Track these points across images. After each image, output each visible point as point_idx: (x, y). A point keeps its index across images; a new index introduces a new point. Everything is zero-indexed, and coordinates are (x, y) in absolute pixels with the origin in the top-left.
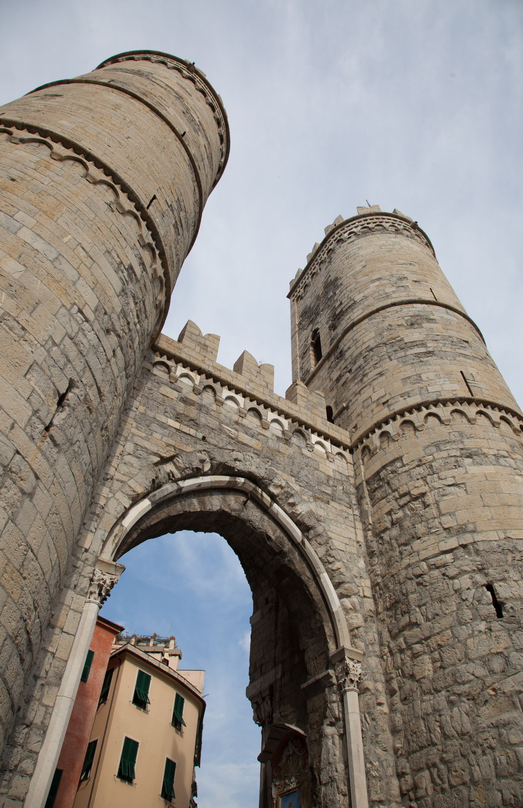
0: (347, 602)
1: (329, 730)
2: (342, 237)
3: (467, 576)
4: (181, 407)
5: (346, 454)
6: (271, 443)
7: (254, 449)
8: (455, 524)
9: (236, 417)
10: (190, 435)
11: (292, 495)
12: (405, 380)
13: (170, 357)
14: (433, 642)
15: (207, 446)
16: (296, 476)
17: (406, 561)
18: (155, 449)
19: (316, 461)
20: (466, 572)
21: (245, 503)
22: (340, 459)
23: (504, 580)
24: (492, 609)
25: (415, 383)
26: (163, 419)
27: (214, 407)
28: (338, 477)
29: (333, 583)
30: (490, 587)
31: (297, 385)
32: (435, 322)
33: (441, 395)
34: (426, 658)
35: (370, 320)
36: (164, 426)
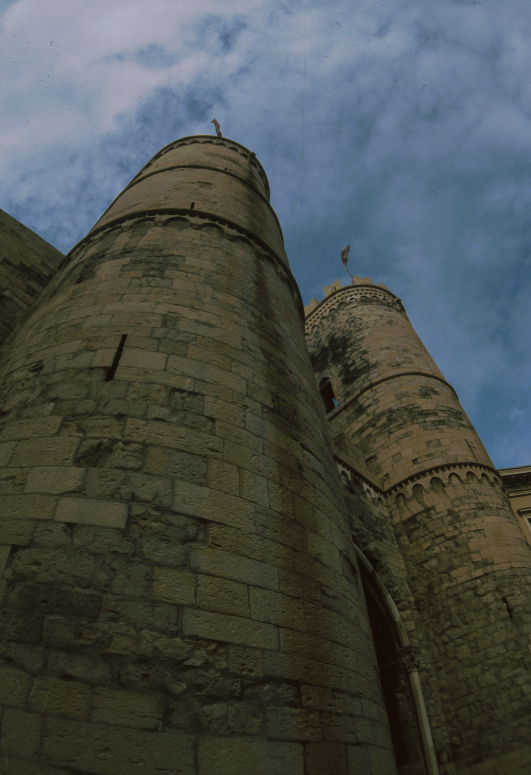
0: (405, 614)
1: (399, 695)
2: (344, 301)
3: (490, 594)
8: (480, 559)
12: (428, 443)
14: (470, 637)
17: (446, 585)
20: (490, 592)
23: (513, 595)
24: (506, 614)
25: (436, 447)
29: (394, 601)
30: (504, 600)
31: (344, 438)
33: (457, 459)
34: (465, 647)
35: (388, 384)
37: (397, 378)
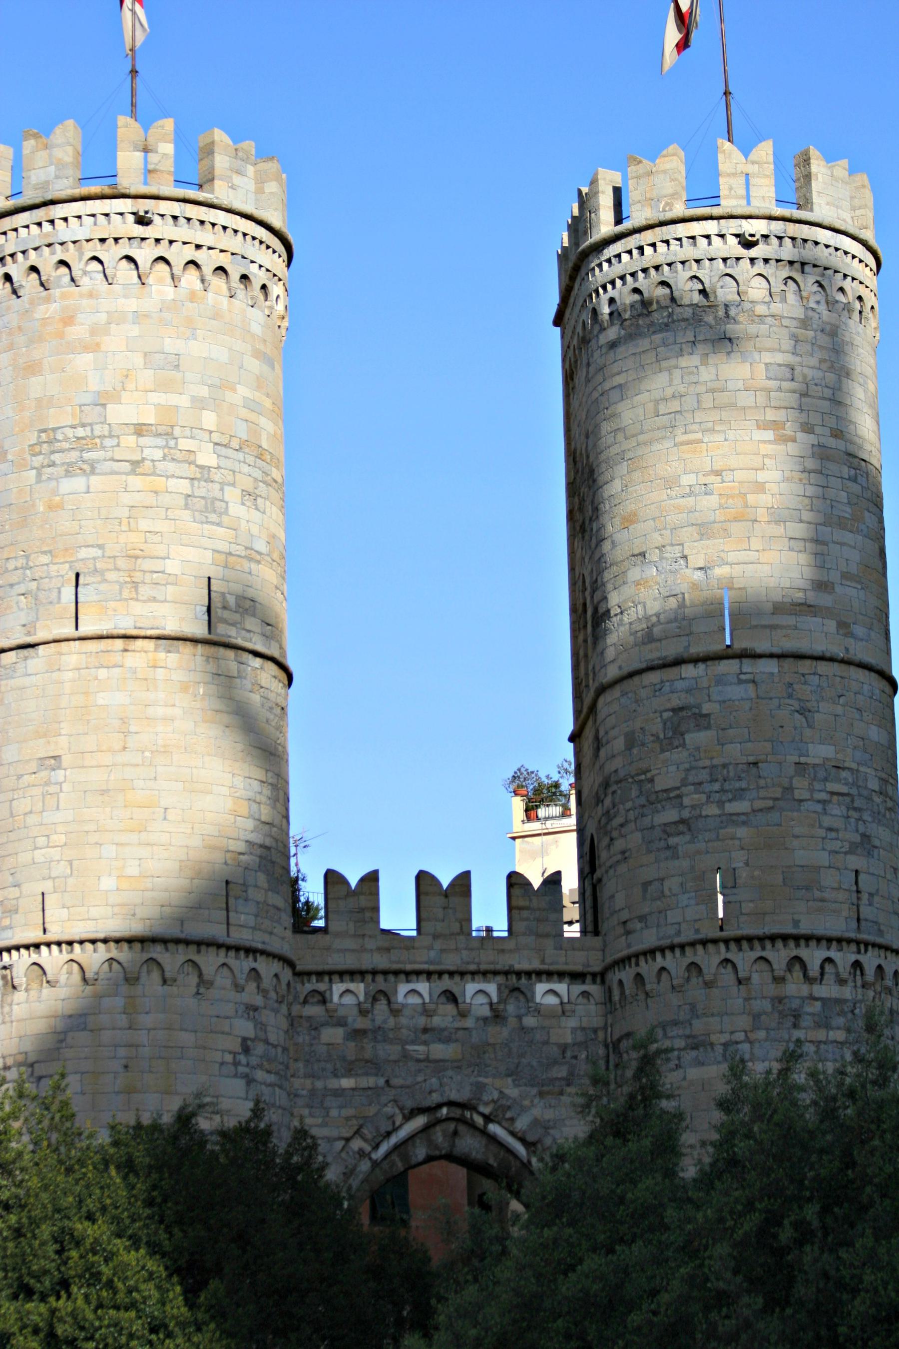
4: (351, 1050)
5: (594, 989)
6: (475, 1039)
7: (452, 1061)
9: (422, 1021)
10: (369, 1088)
11: (509, 1108)
13: (320, 974)
15: (393, 1092)
16: (513, 1073)
18: (335, 1133)
19: (543, 1028)
21: (455, 1133)
22: (585, 1001)
26: (333, 1083)
27: (391, 1022)
28: (580, 1037)
32: (708, 727)
35: (624, 694)
36: (339, 1093)
37: (636, 679)
